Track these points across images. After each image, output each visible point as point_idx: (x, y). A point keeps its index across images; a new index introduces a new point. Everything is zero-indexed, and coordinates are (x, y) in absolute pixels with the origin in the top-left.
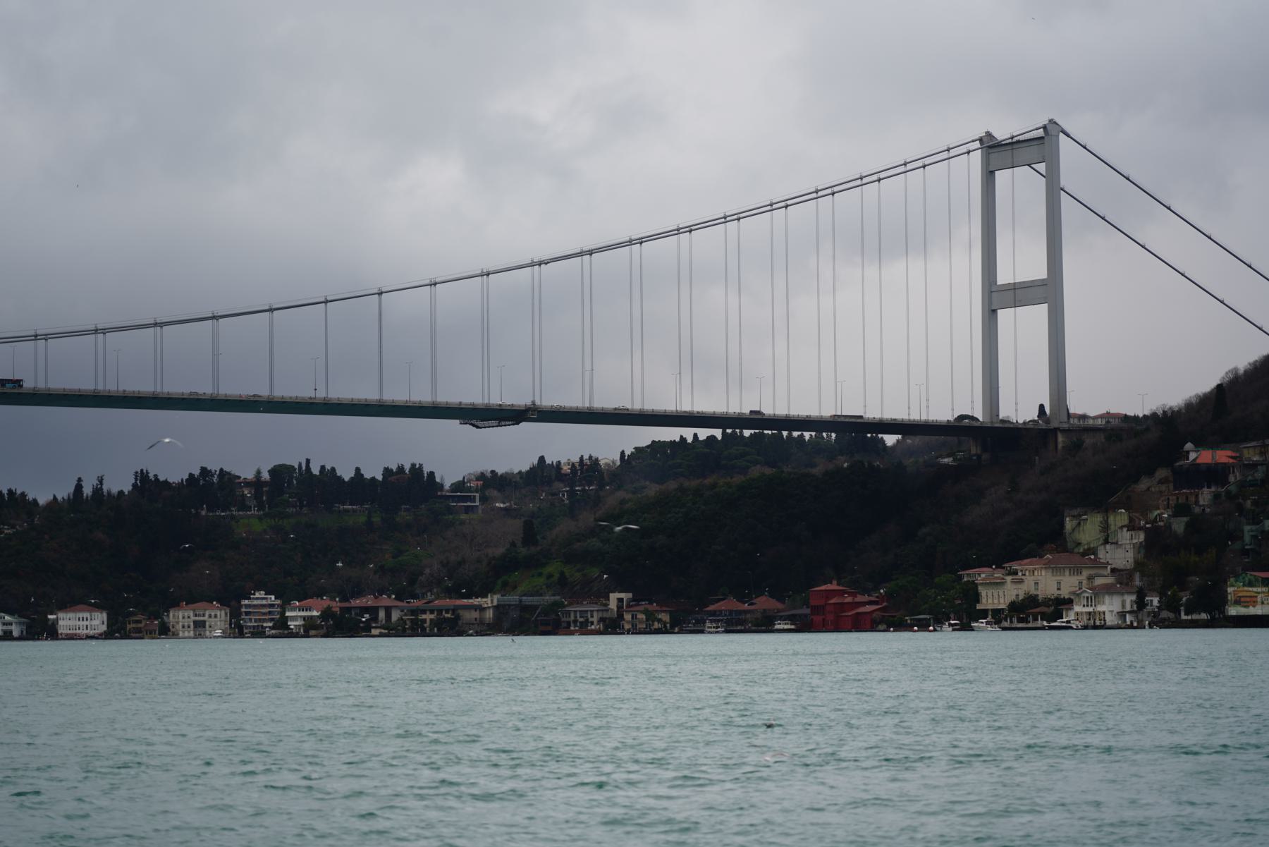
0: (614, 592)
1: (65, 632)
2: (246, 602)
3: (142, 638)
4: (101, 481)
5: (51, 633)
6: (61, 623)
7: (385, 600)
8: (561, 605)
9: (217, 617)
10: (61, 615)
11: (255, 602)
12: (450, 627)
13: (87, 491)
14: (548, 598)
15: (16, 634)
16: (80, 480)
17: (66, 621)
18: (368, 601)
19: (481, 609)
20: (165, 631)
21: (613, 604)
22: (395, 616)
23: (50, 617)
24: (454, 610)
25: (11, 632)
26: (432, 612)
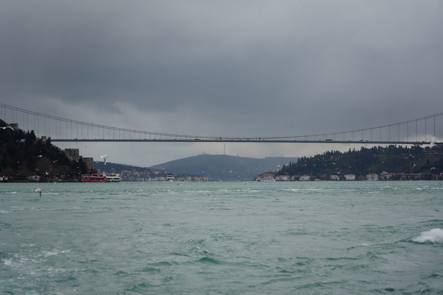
0: (441, 172)
1: (347, 179)
2: (382, 173)
3: (362, 181)
4: (354, 149)
5: (345, 179)
6: (346, 177)
7: (403, 173)
8: (432, 175)
9: (376, 176)
10: (346, 176)
11: (383, 173)
12: (413, 179)
13: (352, 151)
14: (430, 174)
15: (338, 179)
16: (350, 148)
17: (347, 177)
18: (400, 174)
19: (418, 175)
20: (366, 179)
21: (441, 175)
22: (404, 176)
23: (344, 176)
24: (414, 176)
25: (337, 179)
26: (410, 176)
